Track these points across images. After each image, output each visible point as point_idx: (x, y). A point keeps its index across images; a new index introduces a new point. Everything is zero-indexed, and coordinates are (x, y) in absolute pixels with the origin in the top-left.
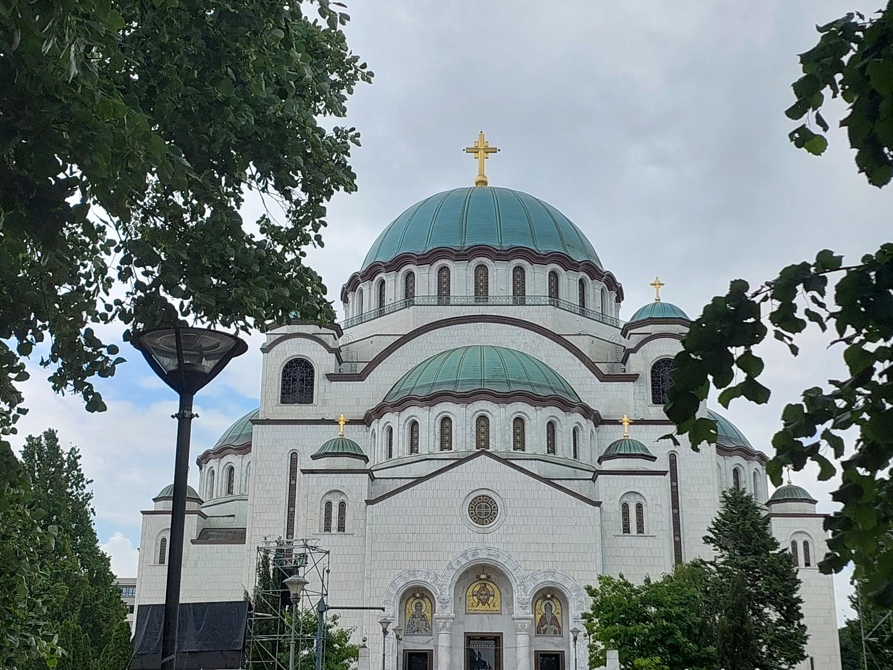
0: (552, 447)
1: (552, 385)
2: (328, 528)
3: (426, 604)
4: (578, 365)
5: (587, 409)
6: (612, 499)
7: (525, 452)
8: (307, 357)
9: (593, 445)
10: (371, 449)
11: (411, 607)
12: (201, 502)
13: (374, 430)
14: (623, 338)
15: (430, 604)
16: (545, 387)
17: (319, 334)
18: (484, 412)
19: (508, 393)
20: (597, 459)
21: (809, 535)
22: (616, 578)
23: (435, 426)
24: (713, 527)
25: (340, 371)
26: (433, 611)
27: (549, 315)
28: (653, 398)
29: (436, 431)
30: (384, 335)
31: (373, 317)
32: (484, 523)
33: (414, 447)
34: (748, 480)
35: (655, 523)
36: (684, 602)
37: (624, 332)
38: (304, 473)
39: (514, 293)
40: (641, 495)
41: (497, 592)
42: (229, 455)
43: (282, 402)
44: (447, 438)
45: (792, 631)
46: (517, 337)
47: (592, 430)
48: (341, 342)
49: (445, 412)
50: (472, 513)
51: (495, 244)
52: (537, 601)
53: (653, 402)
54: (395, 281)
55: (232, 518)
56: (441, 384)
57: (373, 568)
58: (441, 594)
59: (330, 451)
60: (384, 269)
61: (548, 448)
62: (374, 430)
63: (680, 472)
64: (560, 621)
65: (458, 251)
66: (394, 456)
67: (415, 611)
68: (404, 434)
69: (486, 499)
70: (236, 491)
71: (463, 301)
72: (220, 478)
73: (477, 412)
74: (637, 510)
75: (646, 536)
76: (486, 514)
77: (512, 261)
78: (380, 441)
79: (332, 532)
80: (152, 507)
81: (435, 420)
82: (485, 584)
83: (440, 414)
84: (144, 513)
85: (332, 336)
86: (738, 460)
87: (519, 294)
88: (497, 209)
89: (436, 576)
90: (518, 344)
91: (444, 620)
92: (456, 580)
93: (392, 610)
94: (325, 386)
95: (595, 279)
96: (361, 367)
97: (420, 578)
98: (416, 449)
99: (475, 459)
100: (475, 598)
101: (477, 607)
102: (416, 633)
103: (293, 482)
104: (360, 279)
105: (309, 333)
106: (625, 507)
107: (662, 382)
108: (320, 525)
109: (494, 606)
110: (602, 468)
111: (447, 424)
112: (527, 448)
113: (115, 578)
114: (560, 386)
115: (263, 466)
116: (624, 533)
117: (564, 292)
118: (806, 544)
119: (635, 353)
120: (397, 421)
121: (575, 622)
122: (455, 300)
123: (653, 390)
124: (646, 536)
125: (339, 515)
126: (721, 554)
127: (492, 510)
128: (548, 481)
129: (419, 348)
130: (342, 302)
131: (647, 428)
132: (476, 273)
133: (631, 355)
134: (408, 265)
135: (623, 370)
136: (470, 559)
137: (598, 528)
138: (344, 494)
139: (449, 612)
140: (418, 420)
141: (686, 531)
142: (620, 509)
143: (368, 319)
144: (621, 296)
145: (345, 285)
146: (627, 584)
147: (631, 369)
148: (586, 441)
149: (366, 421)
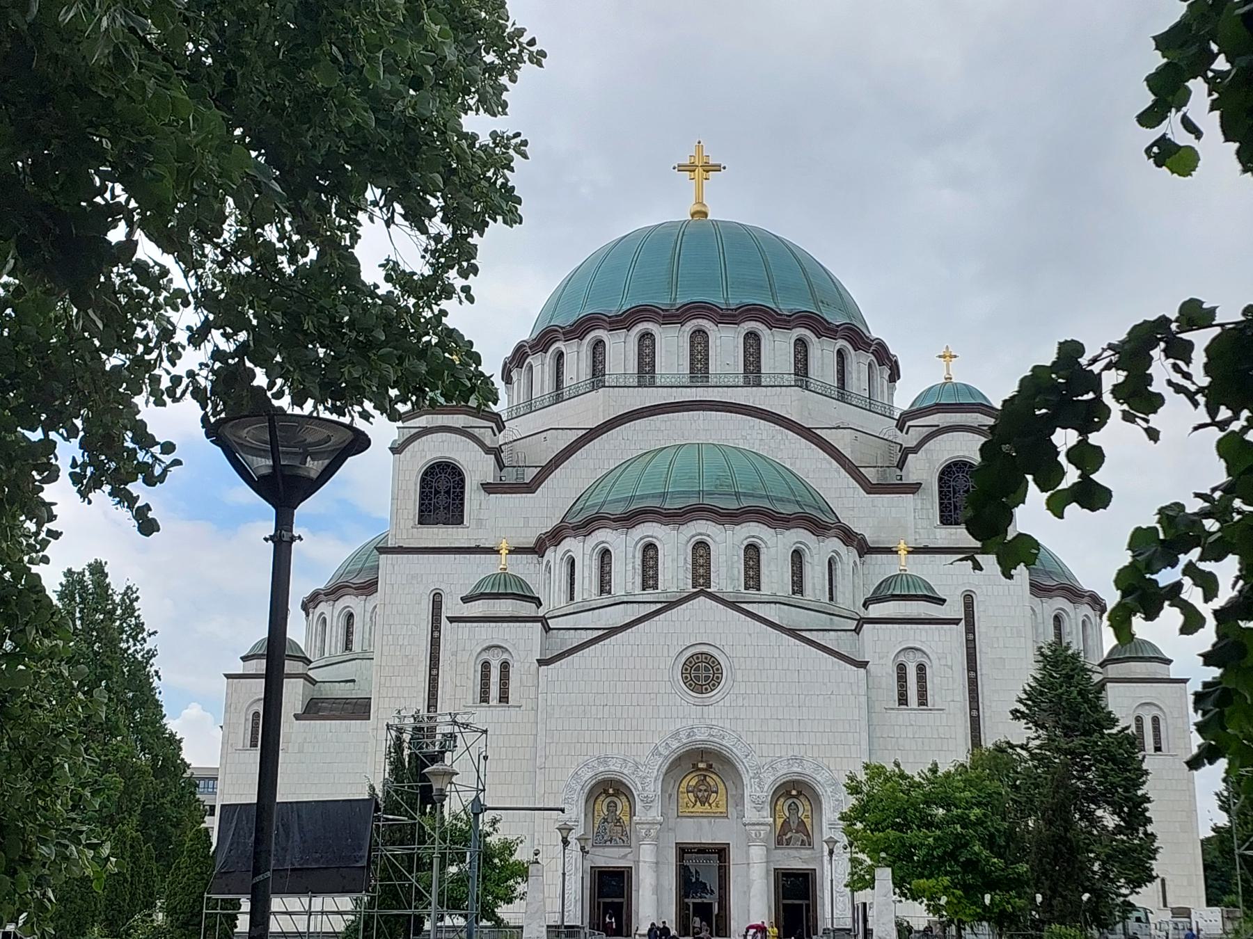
0: (798, 585)
1: (799, 499)
2: (485, 698)
3: (622, 804)
4: (836, 471)
5: (847, 532)
7: (761, 593)
8: (455, 460)
9: (856, 581)
10: (545, 588)
11: (602, 807)
12: (307, 661)
13: (549, 562)
14: (899, 432)
15: (627, 804)
16: (789, 501)
17: (471, 427)
18: (704, 537)
19: (738, 509)
20: (862, 602)
21: (1161, 709)
22: (890, 767)
23: (634, 557)
24: (1025, 696)
25: (501, 480)
26: (632, 813)
27: (795, 401)
28: (941, 517)
29: (637, 563)
30: (562, 429)
31: (546, 404)
32: (704, 691)
33: (604, 585)
34: (1074, 632)
35: (943, 691)
36: (984, 801)
37: (901, 425)
38: (451, 622)
39: (745, 370)
40: (924, 653)
41: (721, 786)
42: (347, 597)
43: (420, 523)
44: (651, 573)
45: (1136, 842)
46: (749, 432)
47: (855, 562)
48: (501, 438)
49: (648, 536)
50: (686, 678)
51: (718, 300)
52: (778, 799)
53: (941, 522)
54: (578, 353)
55: (352, 684)
56: (642, 497)
57: (547, 753)
58: (643, 790)
59: (488, 591)
60: (562, 337)
61: (793, 586)
62: (549, 562)
63: (978, 621)
64: (809, 828)
65: (667, 310)
66: (578, 598)
67: (606, 813)
68: (591, 568)
69: (706, 658)
70: (356, 647)
71: (674, 381)
72: (334, 629)
73: (693, 536)
75: (930, 710)
76: (707, 678)
77: (742, 325)
78: (557, 576)
79: (491, 704)
80: (239, 668)
81: (635, 547)
82: (705, 776)
83: (641, 539)
84: (228, 676)
85: (490, 430)
86: (1060, 603)
87: (753, 371)
88: (721, 251)
89: (636, 765)
90: (751, 441)
91: (648, 826)
92: (664, 771)
93: (575, 812)
94: (481, 500)
95: (860, 349)
96: (530, 474)
97: (613, 768)
98: (608, 588)
99: (691, 602)
101: (693, 807)
102: (608, 843)
103: (436, 634)
104: (528, 350)
105: (458, 426)
106: (902, 669)
107: (955, 493)
108: (474, 692)
110: (868, 614)
111: (651, 553)
112: (763, 586)
113: (189, 768)
114: (810, 501)
115: (395, 612)
116: (899, 704)
117: (816, 367)
118: (1155, 720)
119: (916, 453)
120: (581, 549)
121: (830, 828)
122: (663, 380)
123: (941, 504)
124: (930, 710)
125: (501, 680)
126: (1036, 735)
127: (714, 673)
128: (793, 633)
129: (612, 447)
130: (504, 383)
131: (933, 559)
132: (692, 342)
133: (910, 456)
134: (597, 331)
135: (899, 478)
136: (685, 741)
137: (863, 699)
138: (507, 650)
139: (655, 814)
140: (610, 549)
141: (987, 702)
142: (893, 671)
143: (540, 406)
144: (896, 371)
145: (508, 358)
146: (903, 776)
147: (911, 475)
148: (846, 577)
149: (538, 549)
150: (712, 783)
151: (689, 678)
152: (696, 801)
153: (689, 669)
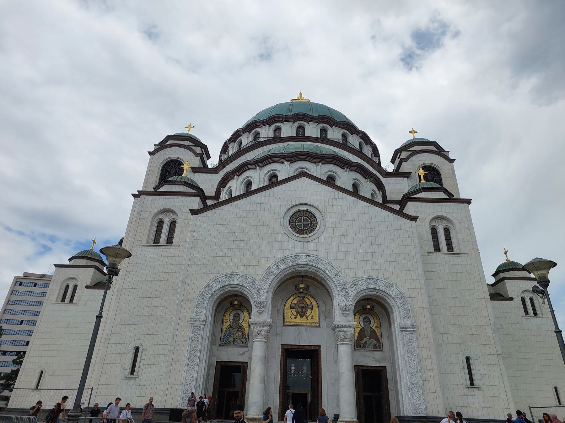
6: (422, 222)
41: (315, 304)
69: (306, 214)
74: (445, 234)
82: (304, 298)
100: (293, 310)
106: (434, 231)
109: (312, 318)
136: (290, 264)
150: (308, 302)
151: (295, 226)
152: (297, 315)
153: (295, 220)
